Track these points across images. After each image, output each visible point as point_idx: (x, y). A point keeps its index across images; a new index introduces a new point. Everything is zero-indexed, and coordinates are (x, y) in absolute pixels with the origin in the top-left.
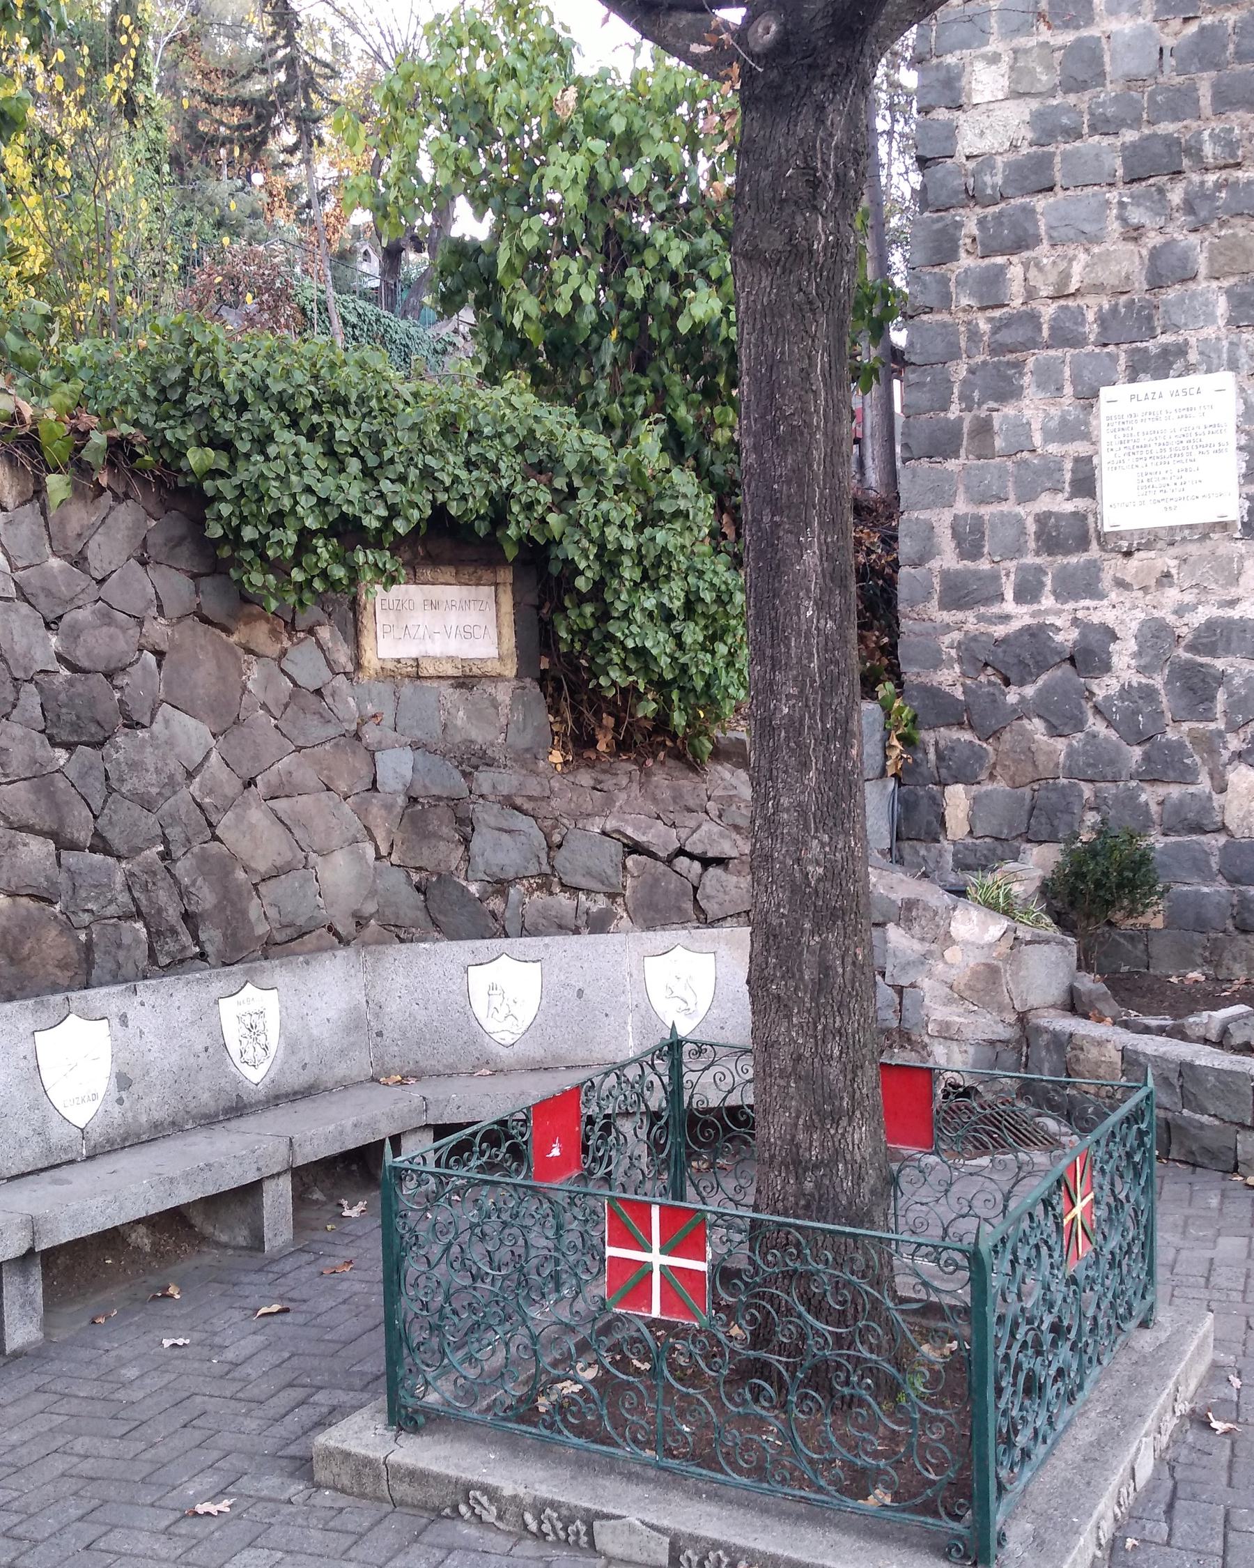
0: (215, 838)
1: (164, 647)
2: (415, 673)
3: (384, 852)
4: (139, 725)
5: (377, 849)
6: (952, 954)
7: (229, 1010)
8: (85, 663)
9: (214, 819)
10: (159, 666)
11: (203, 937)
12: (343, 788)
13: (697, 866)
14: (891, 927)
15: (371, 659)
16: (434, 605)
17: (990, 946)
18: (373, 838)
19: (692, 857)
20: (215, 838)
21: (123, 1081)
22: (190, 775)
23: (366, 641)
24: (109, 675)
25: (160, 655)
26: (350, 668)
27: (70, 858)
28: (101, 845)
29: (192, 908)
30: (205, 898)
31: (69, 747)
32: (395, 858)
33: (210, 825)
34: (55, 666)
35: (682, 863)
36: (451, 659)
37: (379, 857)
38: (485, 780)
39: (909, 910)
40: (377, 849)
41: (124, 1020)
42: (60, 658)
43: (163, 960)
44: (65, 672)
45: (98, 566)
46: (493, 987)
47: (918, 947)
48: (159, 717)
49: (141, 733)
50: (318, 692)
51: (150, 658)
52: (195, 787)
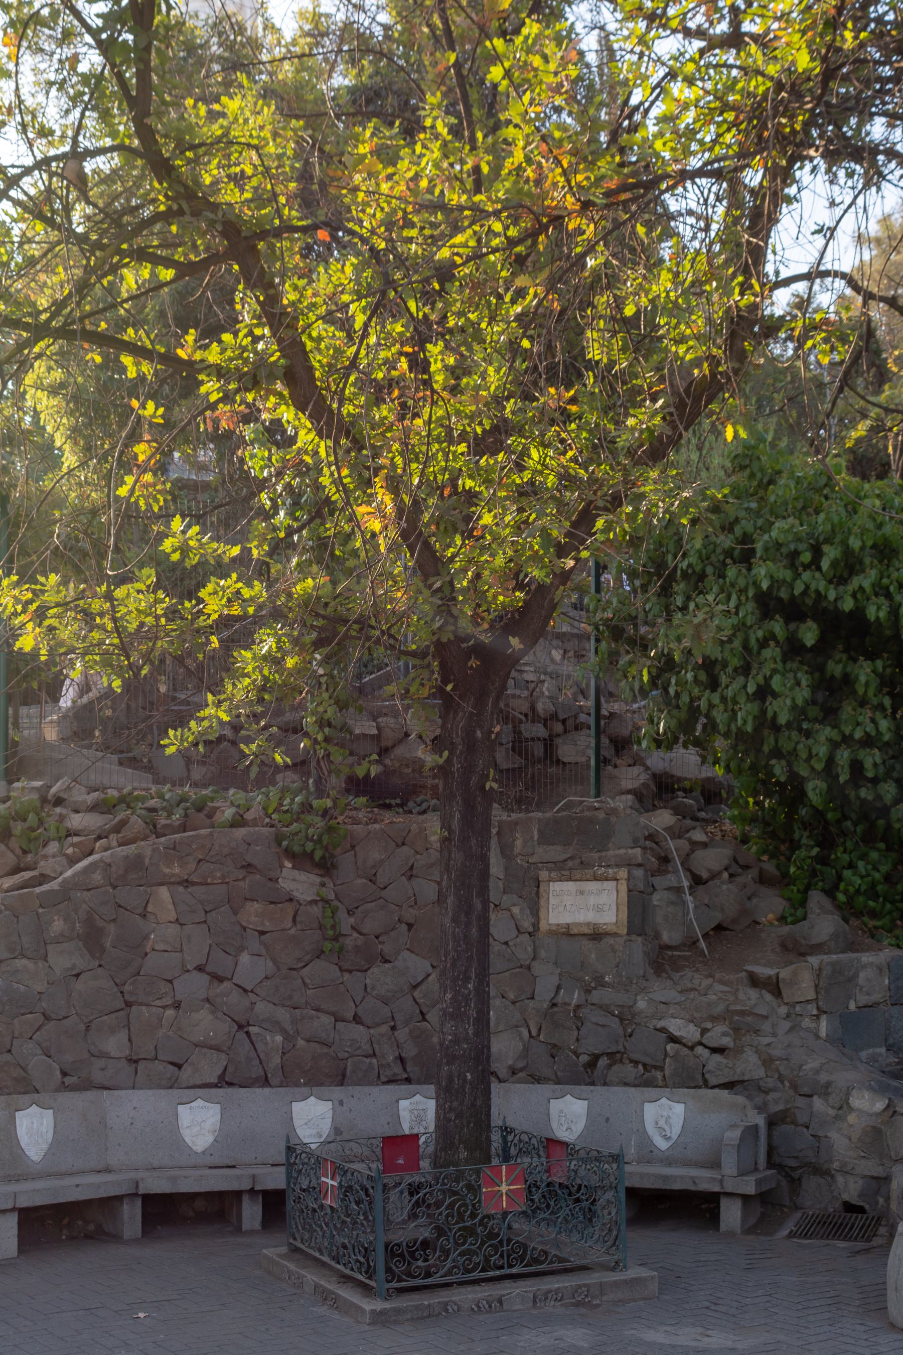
0: (424, 1019)
1: (411, 921)
2: (567, 933)
3: (534, 1033)
4: (387, 961)
5: (530, 1032)
6: (851, 1118)
7: (404, 1104)
8: (364, 931)
9: (424, 1011)
10: (409, 930)
11: (409, 1069)
12: (512, 996)
13: (706, 1052)
14: (815, 1098)
15: (543, 926)
16: (582, 893)
17: (878, 1115)
18: (528, 1026)
19: (706, 1047)
20: (424, 1019)
21: (337, 1130)
22: (415, 987)
23: (542, 914)
24: (377, 937)
25: (410, 926)
26: (531, 929)
27: (340, 1025)
28: (357, 1019)
29: (403, 1055)
30: (410, 1051)
31: (350, 972)
32: (542, 1038)
33: (422, 1012)
34: (349, 931)
35: (699, 1050)
36: (588, 924)
37: (531, 1036)
38: (596, 996)
39: (827, 1087)
40: (530, 1032)
41: (341, 1103)
42: (353, 928)
43: (383, 1079)
44: (355, 935)
45: (381, 880)
46: (561, 1111)
47: (832, 1112)
48: (400, 958)
49: (387, 965)
50: (506, 943)
51: (404, 927)
52: (416, 994)
